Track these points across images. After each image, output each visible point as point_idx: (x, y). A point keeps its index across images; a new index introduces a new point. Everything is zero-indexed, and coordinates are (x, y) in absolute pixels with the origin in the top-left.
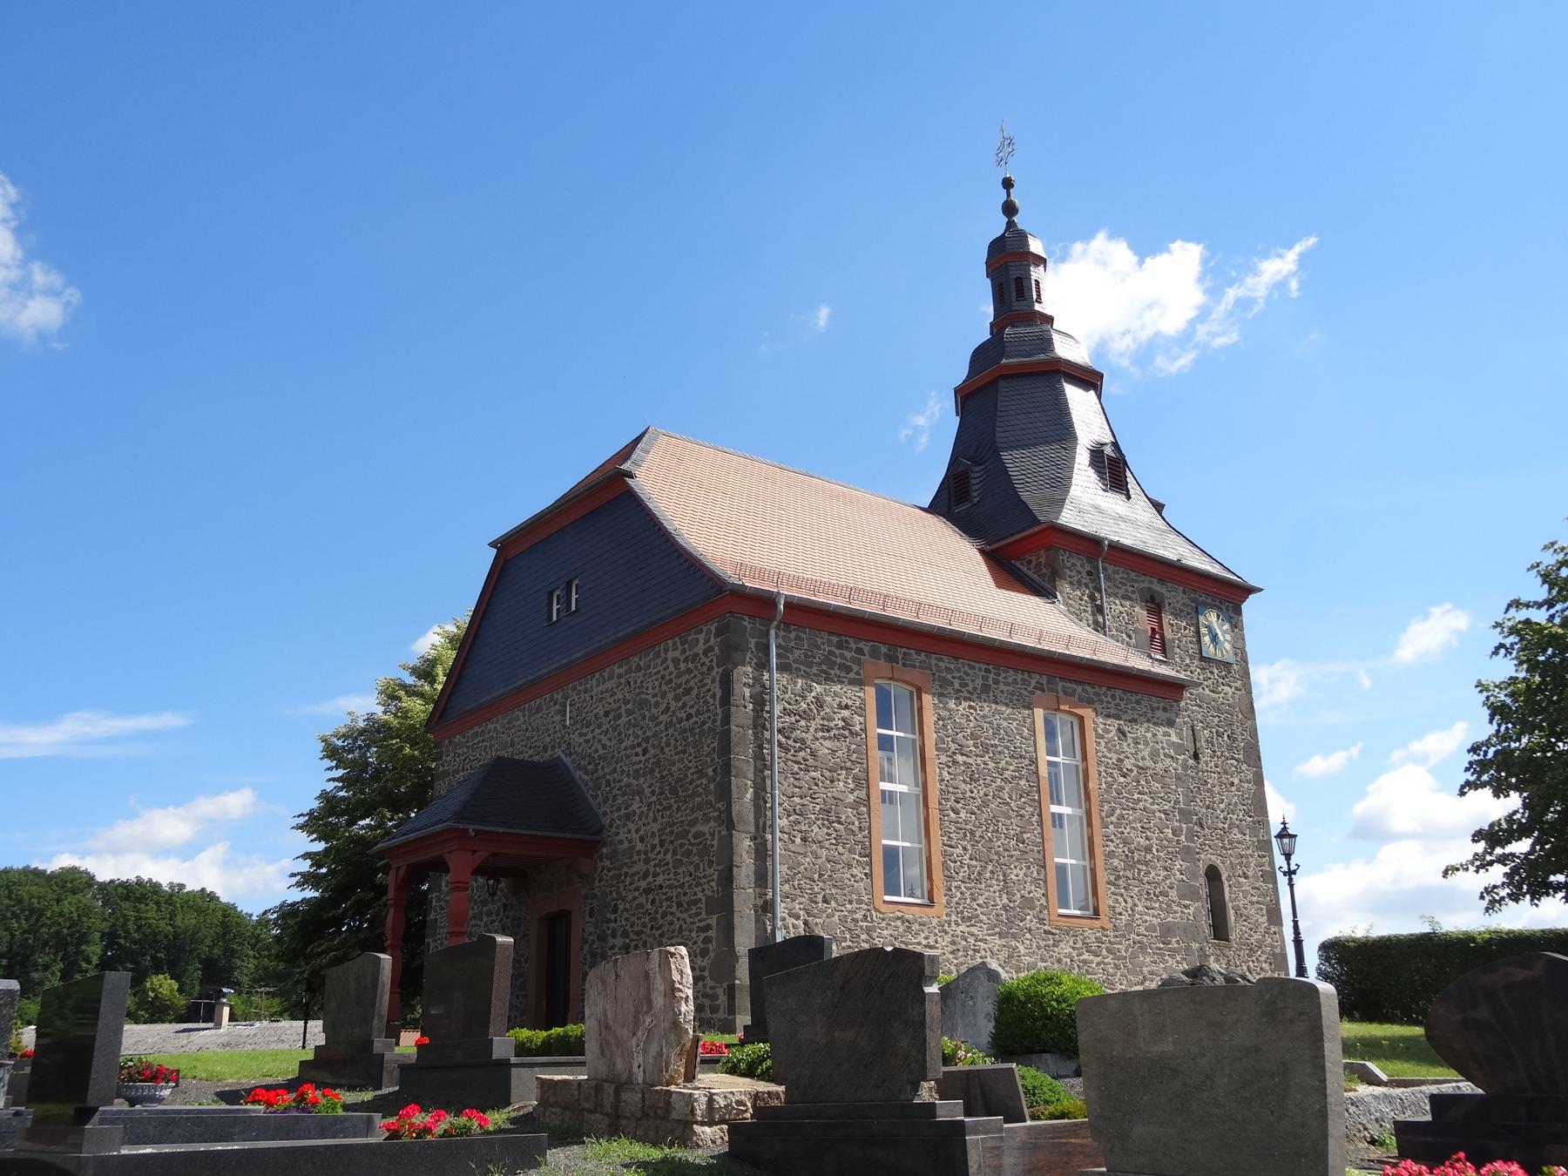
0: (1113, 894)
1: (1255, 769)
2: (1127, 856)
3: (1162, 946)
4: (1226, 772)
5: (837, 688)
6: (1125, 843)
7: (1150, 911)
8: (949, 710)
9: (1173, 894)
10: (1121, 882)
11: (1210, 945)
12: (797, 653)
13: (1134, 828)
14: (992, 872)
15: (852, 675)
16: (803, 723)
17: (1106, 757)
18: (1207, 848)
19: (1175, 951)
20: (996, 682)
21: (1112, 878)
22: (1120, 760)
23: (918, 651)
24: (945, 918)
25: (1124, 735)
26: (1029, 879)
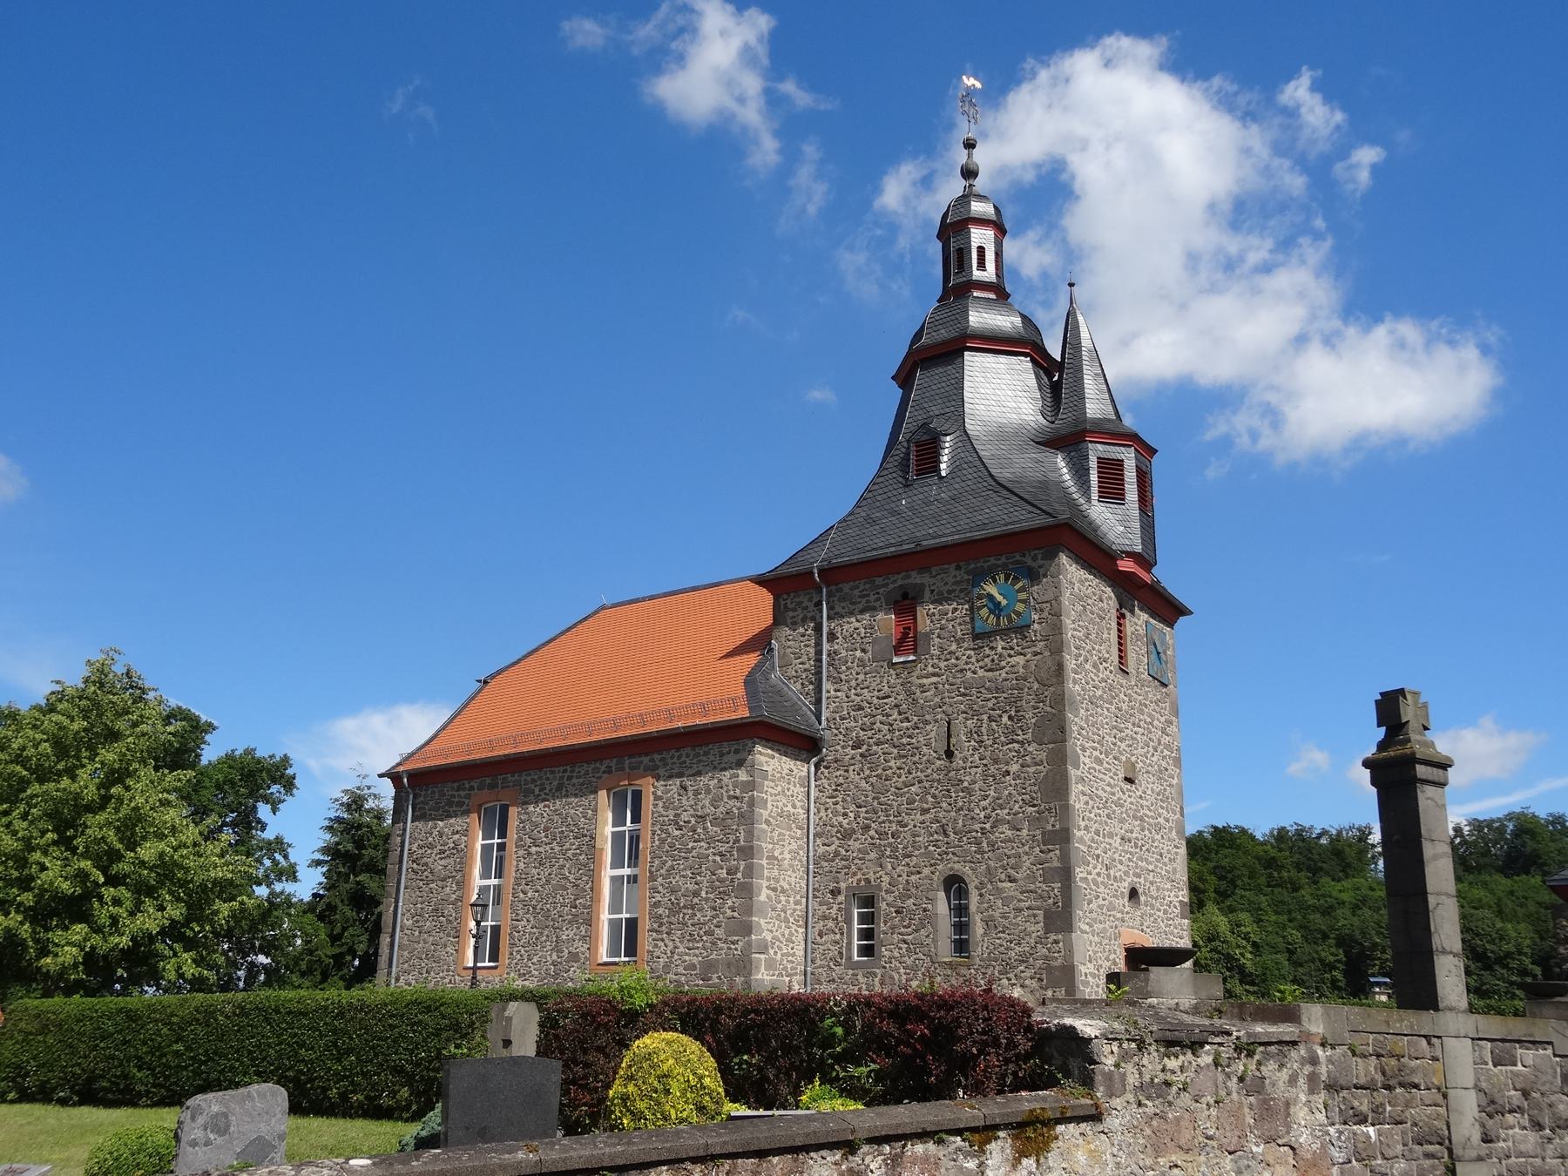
0: (654, 940)
1: (1051, 746)
2: (672, 903)
3: (701, 982)
4: (996, 761)
5: (452, 821)
6: (673, 891)
8: (528, 814)
9: (719, 932)
10: (664, 928)
11: (936, 965)
12: (431, 803)
13: (683, 876)
14: (547, 936)
15: (464, 807)
16: (429, 851)
17: (662, 816)
20: (570, 778)
21: (655, 926)
22: (677, 815)
23: (513, 773)
24: (505, 976)
25: (685, 789)
26: (578, 937)
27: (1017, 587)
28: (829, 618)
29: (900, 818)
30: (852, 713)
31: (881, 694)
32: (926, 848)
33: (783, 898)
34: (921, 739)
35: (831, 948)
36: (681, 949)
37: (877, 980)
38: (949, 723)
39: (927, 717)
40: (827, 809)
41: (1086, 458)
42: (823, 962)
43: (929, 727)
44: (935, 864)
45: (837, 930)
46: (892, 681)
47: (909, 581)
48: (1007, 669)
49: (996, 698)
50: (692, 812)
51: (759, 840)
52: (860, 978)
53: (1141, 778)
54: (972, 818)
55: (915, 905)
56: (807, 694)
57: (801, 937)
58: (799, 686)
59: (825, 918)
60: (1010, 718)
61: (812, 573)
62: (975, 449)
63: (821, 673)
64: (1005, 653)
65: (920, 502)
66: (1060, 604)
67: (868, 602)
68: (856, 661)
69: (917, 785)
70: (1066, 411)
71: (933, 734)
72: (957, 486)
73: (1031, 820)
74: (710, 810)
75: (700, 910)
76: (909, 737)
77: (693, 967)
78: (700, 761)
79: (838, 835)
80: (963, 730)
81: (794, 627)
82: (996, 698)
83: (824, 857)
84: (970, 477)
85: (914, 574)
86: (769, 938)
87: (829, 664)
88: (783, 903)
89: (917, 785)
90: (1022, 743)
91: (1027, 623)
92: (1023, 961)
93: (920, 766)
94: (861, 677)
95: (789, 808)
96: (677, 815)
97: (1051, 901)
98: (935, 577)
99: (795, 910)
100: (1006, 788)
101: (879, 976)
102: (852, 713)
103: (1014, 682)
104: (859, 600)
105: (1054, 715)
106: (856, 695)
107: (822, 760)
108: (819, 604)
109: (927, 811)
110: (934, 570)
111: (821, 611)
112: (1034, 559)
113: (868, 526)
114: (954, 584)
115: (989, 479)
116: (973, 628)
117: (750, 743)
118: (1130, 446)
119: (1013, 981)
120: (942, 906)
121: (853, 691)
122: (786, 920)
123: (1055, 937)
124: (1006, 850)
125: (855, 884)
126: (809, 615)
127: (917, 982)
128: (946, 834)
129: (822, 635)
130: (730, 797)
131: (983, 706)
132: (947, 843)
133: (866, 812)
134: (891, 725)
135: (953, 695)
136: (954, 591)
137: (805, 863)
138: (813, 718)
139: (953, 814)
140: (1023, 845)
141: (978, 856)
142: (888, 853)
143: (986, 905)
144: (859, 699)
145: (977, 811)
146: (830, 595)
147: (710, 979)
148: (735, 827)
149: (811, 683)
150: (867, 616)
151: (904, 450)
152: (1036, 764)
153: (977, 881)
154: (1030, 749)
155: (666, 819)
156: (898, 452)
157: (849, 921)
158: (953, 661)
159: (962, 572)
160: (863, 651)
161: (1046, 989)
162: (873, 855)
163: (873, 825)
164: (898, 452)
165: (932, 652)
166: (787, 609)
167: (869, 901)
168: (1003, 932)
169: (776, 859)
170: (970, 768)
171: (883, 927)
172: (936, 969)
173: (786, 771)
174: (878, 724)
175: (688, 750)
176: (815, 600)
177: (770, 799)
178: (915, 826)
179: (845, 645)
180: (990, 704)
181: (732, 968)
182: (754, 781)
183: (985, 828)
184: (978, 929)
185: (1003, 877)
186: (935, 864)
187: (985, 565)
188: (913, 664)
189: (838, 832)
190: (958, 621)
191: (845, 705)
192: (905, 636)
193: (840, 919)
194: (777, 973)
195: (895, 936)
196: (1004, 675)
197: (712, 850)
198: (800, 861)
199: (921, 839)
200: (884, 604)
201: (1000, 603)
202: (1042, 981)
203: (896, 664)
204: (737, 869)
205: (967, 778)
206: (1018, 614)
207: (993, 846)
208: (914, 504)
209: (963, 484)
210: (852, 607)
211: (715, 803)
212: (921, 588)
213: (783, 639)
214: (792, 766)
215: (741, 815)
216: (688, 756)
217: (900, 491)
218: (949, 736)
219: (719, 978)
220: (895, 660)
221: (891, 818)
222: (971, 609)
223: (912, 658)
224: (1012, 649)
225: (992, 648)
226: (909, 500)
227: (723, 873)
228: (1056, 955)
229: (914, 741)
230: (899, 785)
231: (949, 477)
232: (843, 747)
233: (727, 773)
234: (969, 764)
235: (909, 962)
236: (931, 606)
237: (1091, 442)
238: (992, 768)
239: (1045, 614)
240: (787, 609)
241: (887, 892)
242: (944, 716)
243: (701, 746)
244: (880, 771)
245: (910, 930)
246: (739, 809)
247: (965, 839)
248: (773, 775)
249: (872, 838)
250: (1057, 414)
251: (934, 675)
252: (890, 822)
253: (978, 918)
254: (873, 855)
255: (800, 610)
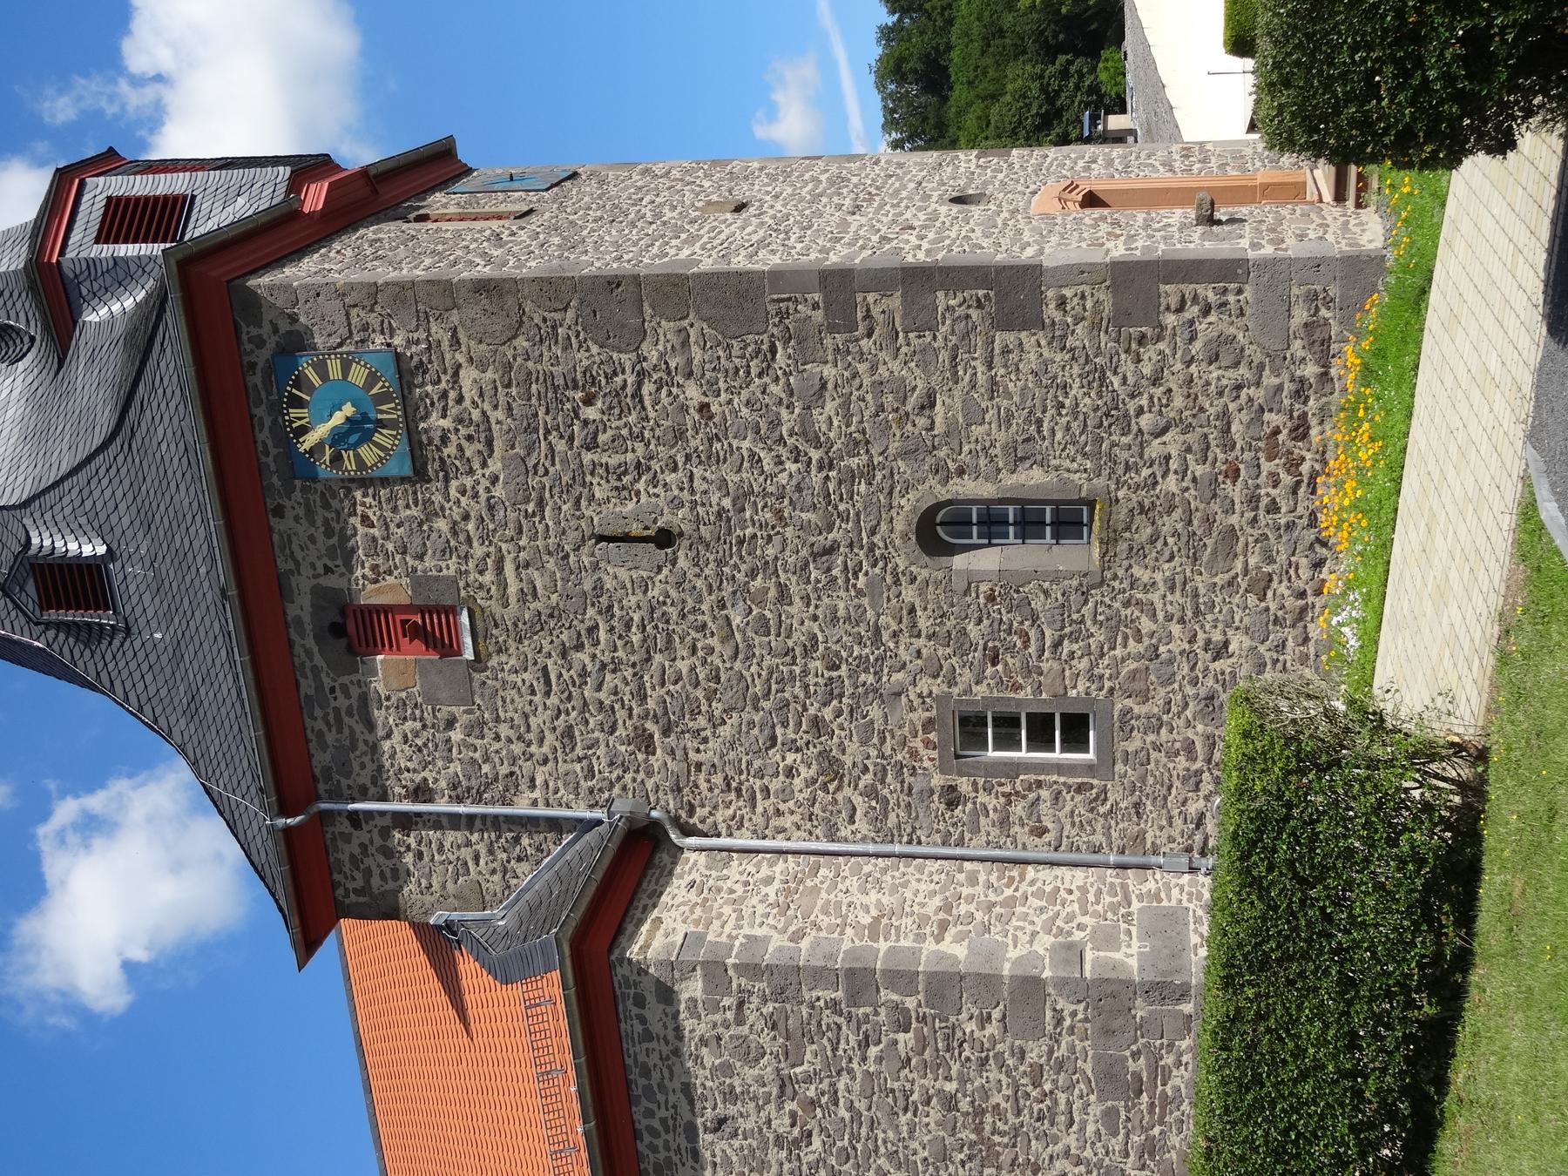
1: (648, 311)
2: (970, 1158)
3: (1145, 1097)
4: (679, 435)
7: (1077, 1119)
9: (1036, 1052)
11: (1108, 574)
13: (911, 1132)
18: (876, 539)
19: (1154, 1067)
22: (779, 1141)
25: (722, 1121)
27: (316, 380)
28: (384, 798)
29: (798, 651)
30: (579, 751)
31: (539, 687)
32: (860, 593)
33: (964, 908)
34: (633, 599)
35: (1068, 808)
36: (1071, 1140)
37: (1136, 709)
38: (601, 538)
39: (587, 586)
40: (778, 813)
41: (91, 263)
42: (1099, 827)
43: (609, 584)
44: (895, 574)
45: (1032, 796)
46: (513, 662)
47: (307, 619)
48: (487, 406)
49: (547, 432)
50: (771, 1107)
51: (832, 956)
52: (1132, 746)
53: (740, 197)
54: (799, 489)
55: (980, 621)
56: (539, 849)
57: (1045, 874)
58: (522, 868)
59: (1004, 822)
60: (589, 401)
61: (287, 830)
62: (56, 484)
63: (496, 817)
64: (454, 411)
65: (157, 600)
66: (352, 287)
67: (350, 713)
68: (471, 740)
69: (729, 611)
70: (12, 313)
71: (623, 574)
72: (126, 521)
73: (803, 358)
74: (767, 1069)
75: (986, 1095)
76: (628, 626)
77: (1110, 1115)
78: (661, 1086)
79: (832, 787)
80: (616, 508)
81: (403, 874)
82: (547, 432)
83: (878, 820)
84: (108, 493)
85: (292, 611)
86: (1049, 940)
87: (479, 800)
88: (972, 908)
89: (729, 611)
90: (641, 375)
91: (390, 358)
92: (1103, 378)
93: (690, 603)
94: (504, 730)
95: (771, 890)
96: (779, 1141)
97: (975, 314)
98: (297, 564)
99: (989, 885)
100: (736, 413)
101: (1129, 702)
102: (579, 751)
103: (514, 391)
104: (346, 731)
105: (582, 302)
106: (541, 741)
107: (676, 821)
108: (355, 819)
109: (783, 590)
110: (283, 565)
111: (369, 814)
112: (260, 342)
113: (201, 711)
114: (312, 523)
115: (113, 449)
116: (403, 480)
117: (621, 971)
118: (82, 185)
119: (1144, 402)
120: (984, 561)
121: (533, 749)
122: (1010, 903)
123: (1052, 306)
124: (867, 414)
125: (935, 754)
126: (378, 841)
127: (1144, 619)
128: (831, 550)
129: (419, 814)
130: (740, 1021)
131: (565, 461)
132: (851, 545)
133: (785, 725)
134: (603, 666)
135: (540, 528)
136: (326, 522)
137: (888, 862)
138: (587, 837)
139: (789, 532)
140: (855, 375)
141: (879, 477)
142: (871, 679)
143: (982, 462)
144: (550, 738)
145: (783, 478)
146: (336, 795)
147: (1138, 1077)
148: (805, 1011)
149: (517, 840)
150: (378, 715)
151: (62, 636)
152: (685, 343)
153: (932, 481)
154: (653, 356)
155: (786, 1166)
156: (66, 650)
157: (1013, 769)
158: (471, 527)
159: (288, 503)
160: (450, 723)
161: (1162, 328)
162: (875, 712)
163: (812, 711)
164: (66, 650)
165: (452, 572)
166: (364, 890)
167: (971, 727)
168: (1039, 423)
169: (877, 920)
170: (692, 492)
171: (1026, 693)
172: (1115, 577)
173: (693, 896)
174: (602, 695)
175: (638, 1112)
176: (344, 826)
177: (747, 931)
178: (815, 618)
179: (440, 763)
180: (561, 446)
181: (1117, 1023)
182: (705, 964)
183: (821, 461)
184: (1032, 479)
185: (922, 422)
186: (895, 574)
187: (273, 451)
188: (478, 615)
189: (825, 788)
190: (388, 514)
191: (562, 767)
192: (417, 633)
193: (1007, 789)
194: (1124, 926)
195: (1045, 666)
196: (500, 414)
197: (855, 1065)
198: (884, 871)
199: (841, 605)
200: (354, 677)
201: (348, 419)
202: (1143, 336)
203: (476, 653)
204: (896, 1007)
205: (714, 500)
206: (372, 379)
207: (857, 443)
208: (160, 613)
209: (122, 507)
210: (362, 747)
211: (752, 1056)
212: (319, 593)
213: (428, 899)
214: (688, 879)
215: (779, 994)
216: (650, 1114)
217: (137, 644)
218: (626, 538)
219: (1136, 1055)
220: (469, 654)
221: (797, 670)
222: (364, 483)
223: (464, 619)
224: (444, 395)
225: (445, 440)
226: (154, 624)
227: (906, 1040)
228: (1089, 304)
229: (636, 617)
230: (728, 652)
231: (108, 538)
232: (650, 774)
233: (688, 1024)
234: (686, 495)
235: (1100, 636)
236: (359, 573)
237: (62, 253)
238: (693, 443)
239: (374, 320)
240: (364, 890)
241: (952, 683)
242: (585, 550)
243: (628, 1084)
244: (700, 693)
245: (1032, 633)
246: (765, 1001)
247: (842, 507)
248: (697, 922)
249: (839, 713)
250: (18, 331)
251: (500, 569)
252: (805, 672)
253: (1009, 480)
254: (875, 712)
255: (368, 861)
